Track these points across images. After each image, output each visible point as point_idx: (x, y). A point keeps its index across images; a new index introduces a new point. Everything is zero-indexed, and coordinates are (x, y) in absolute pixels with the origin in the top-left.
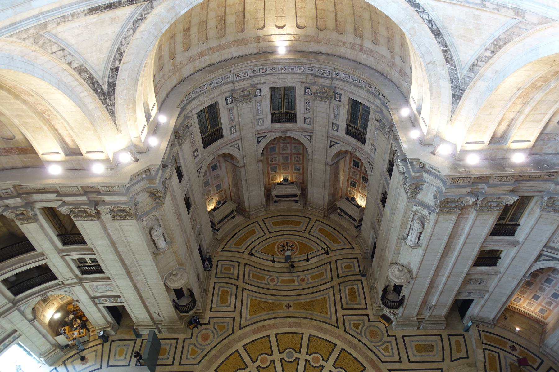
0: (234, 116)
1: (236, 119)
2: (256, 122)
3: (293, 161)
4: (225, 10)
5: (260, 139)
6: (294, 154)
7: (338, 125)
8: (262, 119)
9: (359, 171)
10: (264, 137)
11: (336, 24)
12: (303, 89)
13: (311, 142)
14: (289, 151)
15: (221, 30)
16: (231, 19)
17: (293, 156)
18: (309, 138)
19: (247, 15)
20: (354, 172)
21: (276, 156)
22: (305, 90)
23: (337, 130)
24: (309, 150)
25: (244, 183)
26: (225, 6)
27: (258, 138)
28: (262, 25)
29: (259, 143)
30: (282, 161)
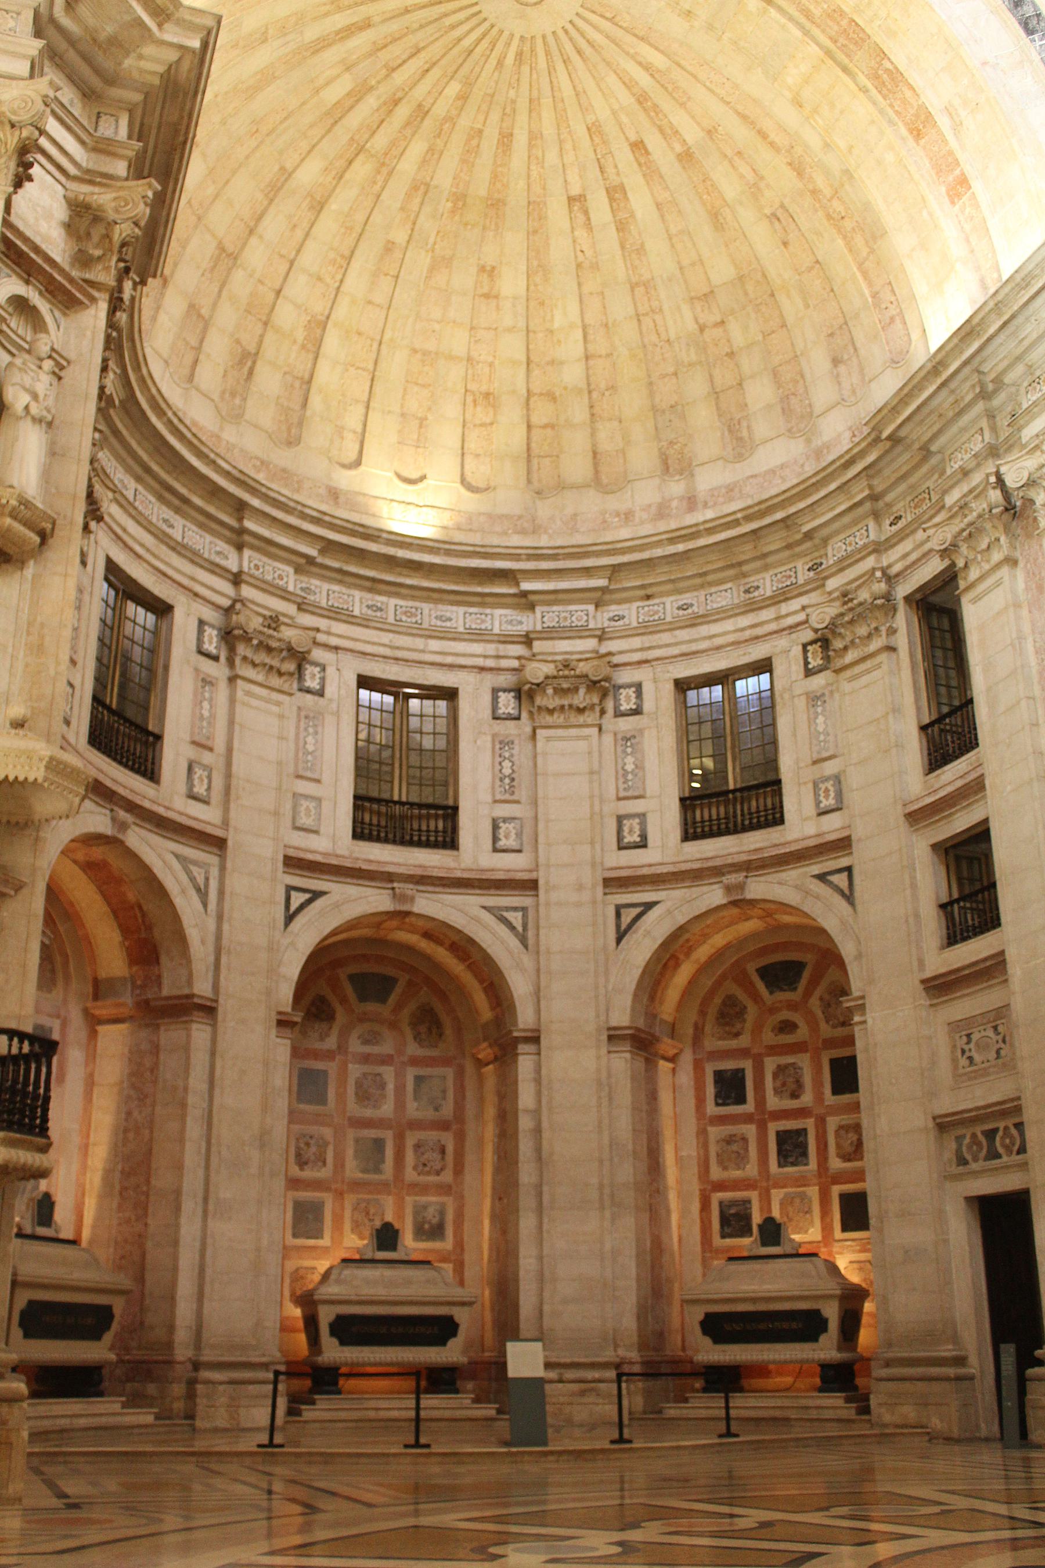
0: (213, 716)
1: (219, 744)
2: (288, 806)
3: (410, 1175)
4: (262, 336)
5: (297, 899)
6: (415, 1125)
7: (642, 816)
8: (319, 800)
9: (748, 1118)
10: (316, 895)
11: (596, 465)
12: (487, 698)
13: (524, 941)
14: (387, 1109)
15: (233, 395)
16: (268, 381)
17: (410, 1140)
18: (516, 918)
19: (316, 401)
20: (729, 1140)
21: (327, 1133)
22: (495, 700)
23: (643, 844)
24: (519, 985)
25: (194, 1130)
26: (266, 324)
27: (290, 889)
28: (353, 456)
29: (290, 918)
30: (352, 1169)
